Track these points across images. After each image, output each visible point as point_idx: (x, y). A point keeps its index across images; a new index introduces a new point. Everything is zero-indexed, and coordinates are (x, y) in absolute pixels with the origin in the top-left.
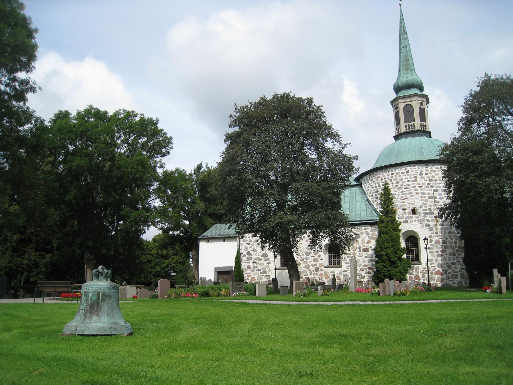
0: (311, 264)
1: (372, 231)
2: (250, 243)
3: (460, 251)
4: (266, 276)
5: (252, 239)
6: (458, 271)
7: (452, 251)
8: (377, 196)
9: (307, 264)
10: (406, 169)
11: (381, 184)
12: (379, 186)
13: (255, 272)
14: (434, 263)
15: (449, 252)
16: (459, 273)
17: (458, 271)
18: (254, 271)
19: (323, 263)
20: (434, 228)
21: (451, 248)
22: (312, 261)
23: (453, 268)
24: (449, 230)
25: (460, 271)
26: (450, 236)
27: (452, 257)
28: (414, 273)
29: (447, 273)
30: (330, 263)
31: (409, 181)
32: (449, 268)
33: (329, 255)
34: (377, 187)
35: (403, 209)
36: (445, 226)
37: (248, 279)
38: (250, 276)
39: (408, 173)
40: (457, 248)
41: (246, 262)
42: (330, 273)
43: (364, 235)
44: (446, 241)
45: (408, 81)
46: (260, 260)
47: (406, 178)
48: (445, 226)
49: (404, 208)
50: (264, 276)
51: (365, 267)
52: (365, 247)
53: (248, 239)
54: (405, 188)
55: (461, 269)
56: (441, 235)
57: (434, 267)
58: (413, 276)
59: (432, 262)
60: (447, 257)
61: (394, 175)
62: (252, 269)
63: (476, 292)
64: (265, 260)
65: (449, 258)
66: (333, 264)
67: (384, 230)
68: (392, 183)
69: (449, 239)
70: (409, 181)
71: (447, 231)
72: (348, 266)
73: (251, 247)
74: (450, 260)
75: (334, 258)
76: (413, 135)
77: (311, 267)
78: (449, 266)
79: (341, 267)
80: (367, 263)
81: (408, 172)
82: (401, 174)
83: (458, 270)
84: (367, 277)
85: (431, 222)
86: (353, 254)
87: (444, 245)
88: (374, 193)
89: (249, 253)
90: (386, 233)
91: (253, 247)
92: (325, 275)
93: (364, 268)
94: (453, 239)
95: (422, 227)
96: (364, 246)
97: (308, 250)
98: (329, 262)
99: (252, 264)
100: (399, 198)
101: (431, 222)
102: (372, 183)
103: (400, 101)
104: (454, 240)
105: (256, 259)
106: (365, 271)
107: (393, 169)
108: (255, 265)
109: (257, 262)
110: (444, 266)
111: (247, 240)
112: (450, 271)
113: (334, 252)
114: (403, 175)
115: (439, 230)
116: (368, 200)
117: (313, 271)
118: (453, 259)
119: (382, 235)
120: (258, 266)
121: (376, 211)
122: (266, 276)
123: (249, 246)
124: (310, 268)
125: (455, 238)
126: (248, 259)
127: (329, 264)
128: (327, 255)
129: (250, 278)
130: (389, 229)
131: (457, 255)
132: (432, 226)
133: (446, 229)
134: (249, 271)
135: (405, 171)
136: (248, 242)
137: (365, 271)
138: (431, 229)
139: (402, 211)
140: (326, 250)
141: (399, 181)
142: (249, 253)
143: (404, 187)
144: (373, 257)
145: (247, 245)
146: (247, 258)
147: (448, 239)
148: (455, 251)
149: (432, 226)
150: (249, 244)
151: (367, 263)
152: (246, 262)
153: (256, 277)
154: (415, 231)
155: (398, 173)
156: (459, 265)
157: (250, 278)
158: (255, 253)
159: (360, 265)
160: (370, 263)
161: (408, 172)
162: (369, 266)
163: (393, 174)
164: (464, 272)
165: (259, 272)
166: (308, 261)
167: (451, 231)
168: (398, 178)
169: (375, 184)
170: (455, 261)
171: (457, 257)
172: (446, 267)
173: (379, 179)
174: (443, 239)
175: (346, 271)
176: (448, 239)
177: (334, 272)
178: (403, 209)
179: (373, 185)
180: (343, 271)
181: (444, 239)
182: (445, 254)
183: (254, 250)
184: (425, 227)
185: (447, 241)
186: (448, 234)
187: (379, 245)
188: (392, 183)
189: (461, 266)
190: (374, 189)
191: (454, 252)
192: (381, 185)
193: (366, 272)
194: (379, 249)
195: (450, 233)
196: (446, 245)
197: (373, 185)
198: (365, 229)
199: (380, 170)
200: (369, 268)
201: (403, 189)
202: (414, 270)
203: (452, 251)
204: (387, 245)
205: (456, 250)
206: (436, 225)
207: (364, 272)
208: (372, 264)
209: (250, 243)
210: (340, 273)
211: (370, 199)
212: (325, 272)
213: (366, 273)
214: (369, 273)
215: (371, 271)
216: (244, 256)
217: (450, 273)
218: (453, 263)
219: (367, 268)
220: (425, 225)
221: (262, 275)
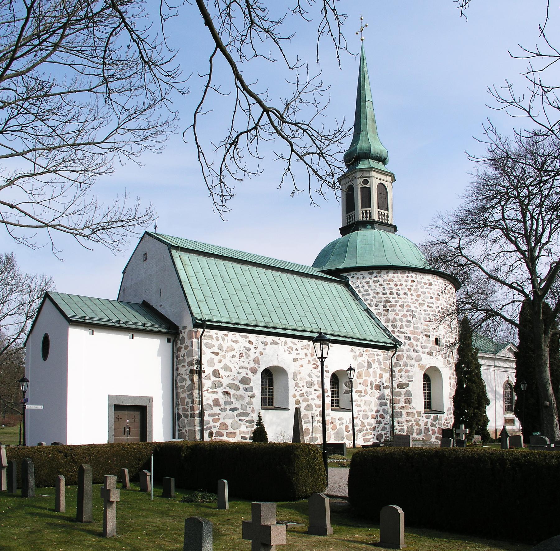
0: (315, 404)
1: (385, 359)
2: (220, 352)
4: (247, 422)
5: (223, 345)
8: (388, 308)
9: (309, 403)
10: (429, 280)
11: (395, 292)
12: (391, 293)
13: (228, 412)
18: (225, 409)
22: (316, 398)
28: (437, 425)
31: (432, 298)
34: (388, 295)
35: (426, 335)
37: (215, 427)
38: (219, 419)
39: (431, 287)
41: (210, 390)
42: (337, 421)
43: (376, 363)
45: (381, 151)
46: (237, 389)
47: (429, 293)
49: (427, 334)
50: (244, 422)
52: (377, 383)
53: (216, 344)
54: (428, 306)
58: (436, 429)
61: (414, 284)
62: (223, 407)
64: (246, 390)
68: (412, 295)
70: (432, 298)
73: (220, 361)
76: (387, 228)
77: (314, 408)
81: (431, 284)
82: (423, 285)
88: (381, 302)
89: (216, 373)
91: (224, 361)
92: (332, 423)
96: (376, 380)
97: (310, 379)
99: (222, 395)
100: (422, 318)
102: (376, 286)
103: (374, 174)
105: (230, 386)
107: (414, 275)
108: (227, 398)
109: (232, 392)
111: (213, 346)
114: (425, 286)
116: (367, 310)
117: (317, 416)
120: (233, 399)
121: (385, 330)
122: (247, 422)
123: (216, 358)
124: (314, 411)
126: (216, 385)
129: (217, 424)
134: (216, 410)
135: (428, 282)
136: (216, 349)
137: (377, 419)
139: (425, 338)
141: (421, 293)
142: (216, 373)
143: (426, 304)
145: (213, 356)
146: (214, 383)
150: (217, 354)
152: (210, 390)
153: (229, 422)
155: (419, 283)
157: (217, 424)
158: (227, 374)
161: (431, 284)
163: (413, 281)
165: (235, 413)
166: (310, 397)
168: (420, 290)
169: (384, 289)
173: (392, 285)
178: (426, 335)
179: (380, 289)
183: (227, 368)
188: (412, 295)
190: (381, 295)
192: (395, 294)
197: (380, 289)
198: (378, 355)
199: (393, 269)
201: (425, 307)
202: (437, 421)
209: (220, 352)
211: (372, 309)
212: (332, 418)
216: (208, 377)
221: (241, 420)
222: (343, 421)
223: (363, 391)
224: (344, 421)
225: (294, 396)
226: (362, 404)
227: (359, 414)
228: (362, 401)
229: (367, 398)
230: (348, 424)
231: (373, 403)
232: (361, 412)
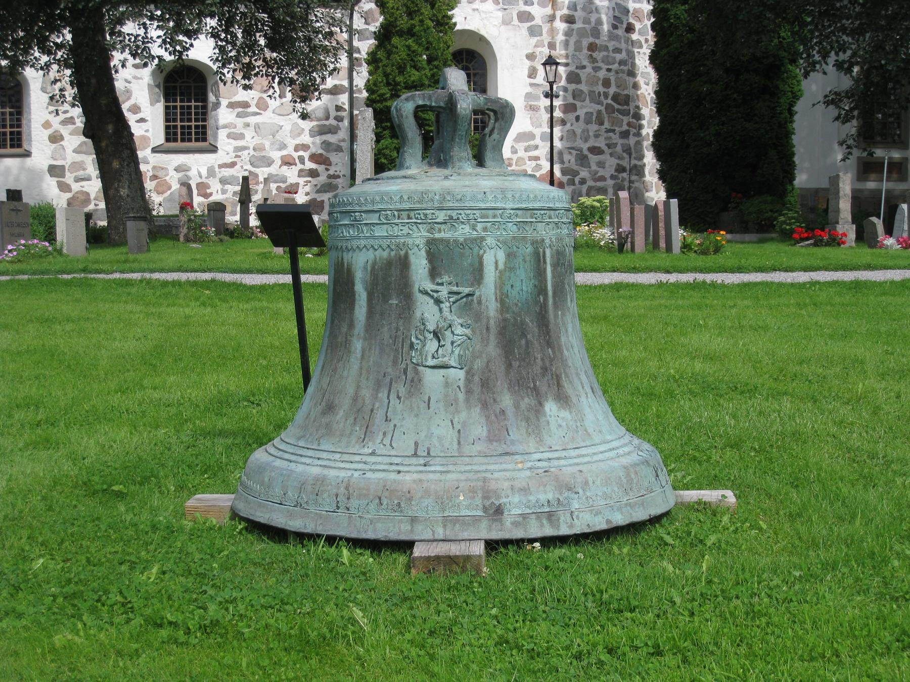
3: (619, 111)
6: (608, 176)
7: (593, 108)
14: (536, 147)
15: (585, 111)
16: (610, 182)
17: (608, 176)
19: (149, 134)
20: (545, 28)
21: (592, 101)
23: (594, 167)
24: (591, 40)
25: (613, 177)
26: (593, 60)
27: (593, 127)
29: (577, 180)
30: (170, 135)
32: (582, 165)
33: (167, 108)
36: (579, 25)
40: (609, 101)
44: (578, 75)
48: (579, 25)
51: (301, 153)
55: (616, 170)
56: (563, 52)
57: (537, 158)
59: (532, 143)
60: (579, 128)
63: (756, 245)
65: (583, 131)
66: (183, 140)
67: (403, 22)
69: (589, 70)
71: (585, 43)
72: (238, 149)
74: (586, 140)
75: (186, 114)
78: (582, 160)
79: (213, 149)
80: (306, 139)
83: (608, 171)
84: (308, 189)
85: (536, 6)
86: (257, 106)
87: (572, 87)
90: (410, 33)
93: (296, 155)
94: (600, 68)
95: (506, 22)
98: (167, 134)
101: (536, 6)
104: (602, 74)
106: (300, 166)
110: (566, 157)
112: (584, 173)
113: (186, 95)
115: (560, 38)
118: (597, 136)
119: (395, 40)
125: (605, 67)
127: (168, 140)
128: (160, 107)
130: (422, 21)
131: (607, 125)
132: (538, 21)
133: (582, 33)
137: (300, 166)
138: (534, 31)
140: (158, 86)
144: (327, 118)
147: (584, 67)
148: (603, 108)
149: (538, 21)
151: (306, 139)
154: (483, 32)
156: (611, 155)
159: (283, 146)
160: (318, 140)
162: (313, 150)
164: (623, 180)
167: (597, 41)
170: (601, 143)
171: (608, 131)
172: (573, 160)
174: (569, 68)
175: (232, 165)
176: (584, 67)
177: (189, 169)
180: (220, 166)
181: (572, 68)
182: (571, 116)
184: (516, 21)
185: (583, 74)
186: (585, 51)
187: (386, 75)
189: (617, 161)
191: (599, 112)
193: (301, 171)
194: (385, 90)
195: (592, 47)
196: (579, 86)
200: (314, 158)
203: (593, 108)
204: (415, 75)
205: (608, 106)
206: (552, 19)
207: (295, 170)
208: (324, 142)
210: (211, 173)
212: (154, 168)
213: (301, 173)
214: (313, 173)
215: (321, 168)
217: (583, 182)
218: (595, 150)
219: (306, 155)
220: (515, 17)
222: (188, 173)
223: (253, 103)
224: (193, 173)
225: (47, 125)
226: (249, 134)
227: (237, 156)
228: (247, 125)
229: (267, 117)
230: (204, 180)
231: (287, 127)
232: (246, 152)
